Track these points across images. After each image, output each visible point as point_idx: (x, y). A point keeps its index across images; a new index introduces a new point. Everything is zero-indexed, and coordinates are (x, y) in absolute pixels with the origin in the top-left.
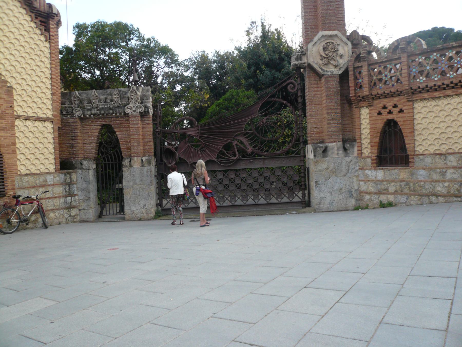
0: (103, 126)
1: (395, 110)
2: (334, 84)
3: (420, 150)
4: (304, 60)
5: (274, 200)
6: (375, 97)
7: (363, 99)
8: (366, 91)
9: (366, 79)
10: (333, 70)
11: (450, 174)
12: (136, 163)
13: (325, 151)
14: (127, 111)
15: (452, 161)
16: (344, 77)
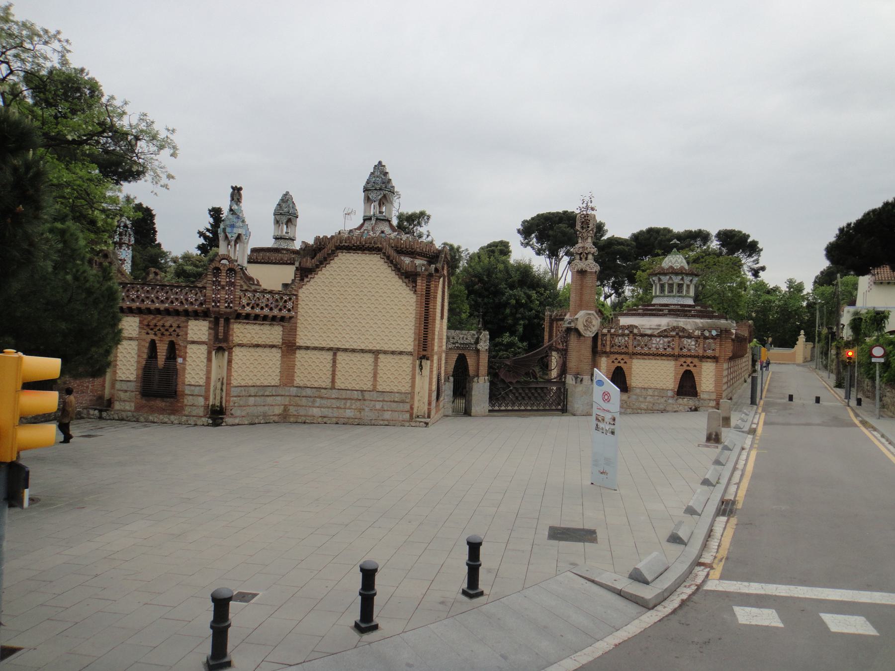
0: (460, 355)
1: (622, 362)
2: (589, 343)
3: (633, 385)
4: (573, 325)
5: (510, 408)
6: (612, 353)
7: (605, 353)
8: (608, 350)
9: (608, 343)
10: (590, 334)
11: (649, 399)
12: (481, 379)
13: (581, 380)
14: (479, 347)
15: (650, 392)
16: (595, 338)
